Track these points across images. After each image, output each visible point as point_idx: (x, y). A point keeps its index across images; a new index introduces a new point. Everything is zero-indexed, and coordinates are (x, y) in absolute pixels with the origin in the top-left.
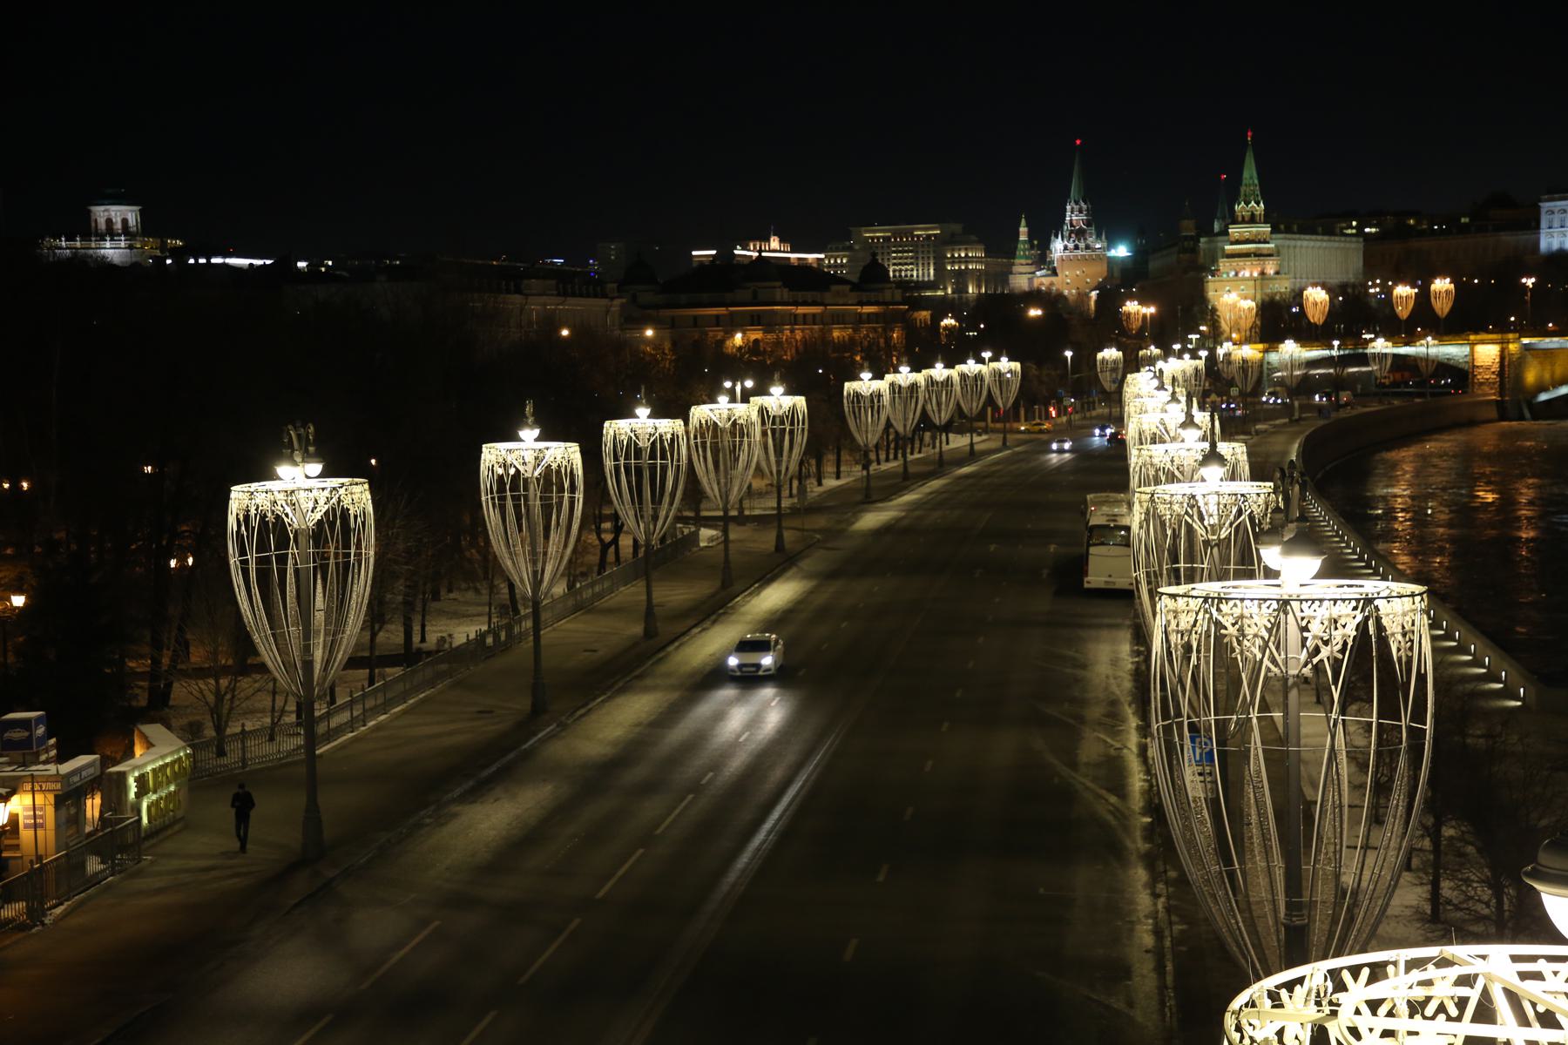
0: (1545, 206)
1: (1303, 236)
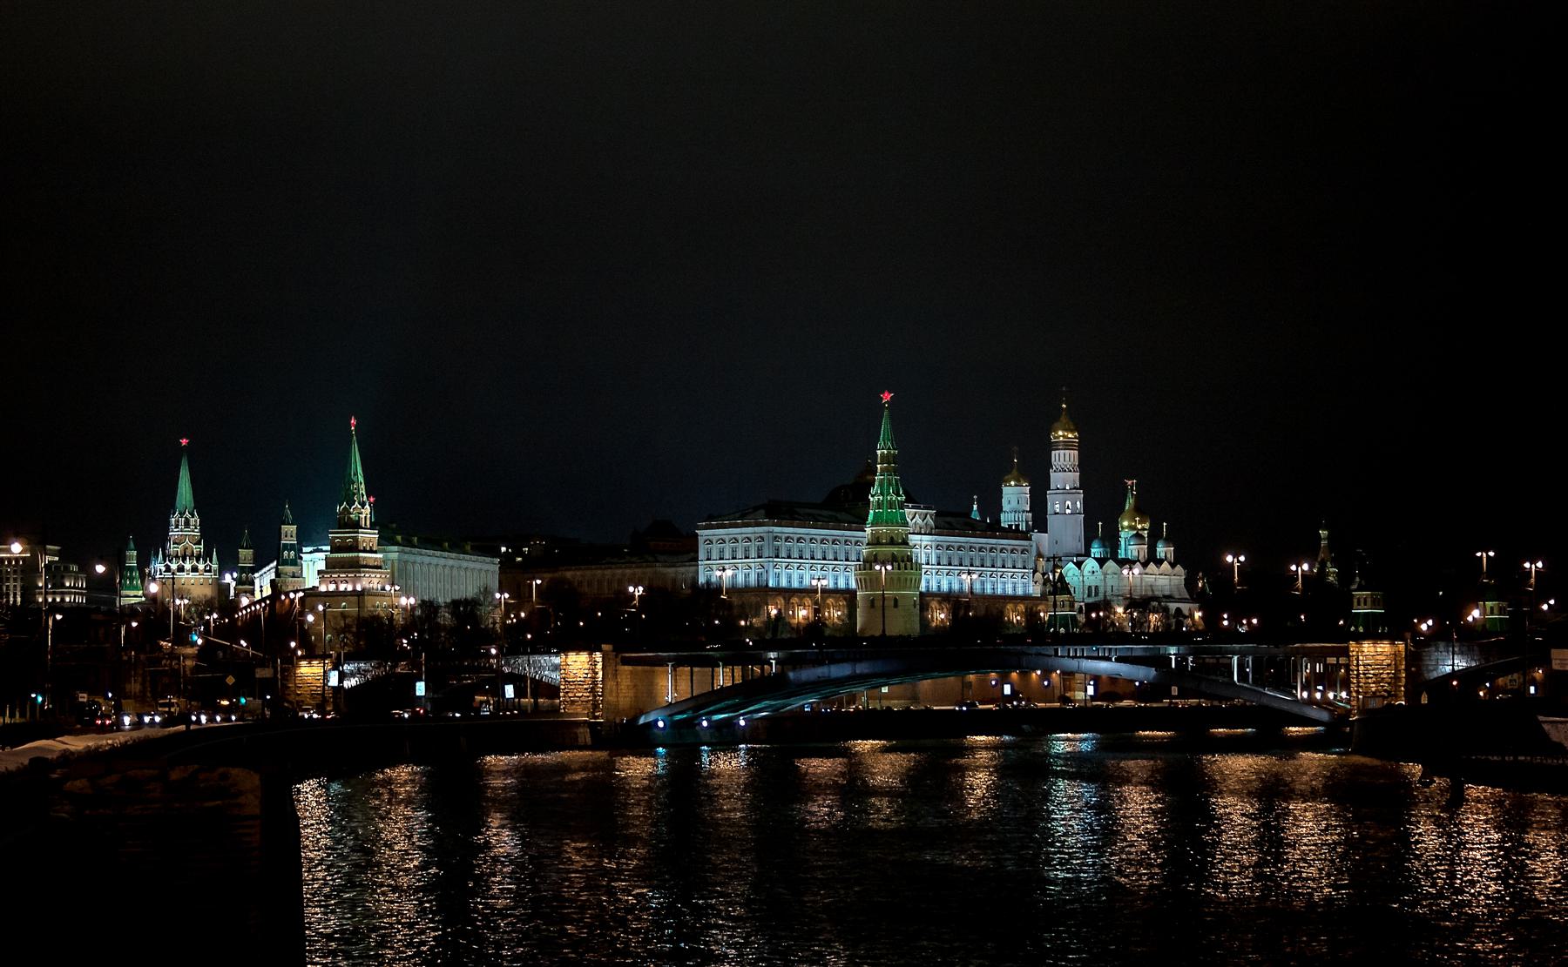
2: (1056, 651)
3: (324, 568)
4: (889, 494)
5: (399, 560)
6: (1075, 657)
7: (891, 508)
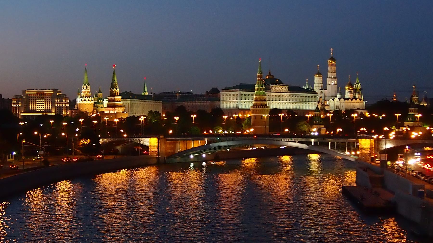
0: (222, 93)
2: (282, 139)
4: (260, 87)
5: (130, 103)
6: (287, 141)
7: (261, 91)
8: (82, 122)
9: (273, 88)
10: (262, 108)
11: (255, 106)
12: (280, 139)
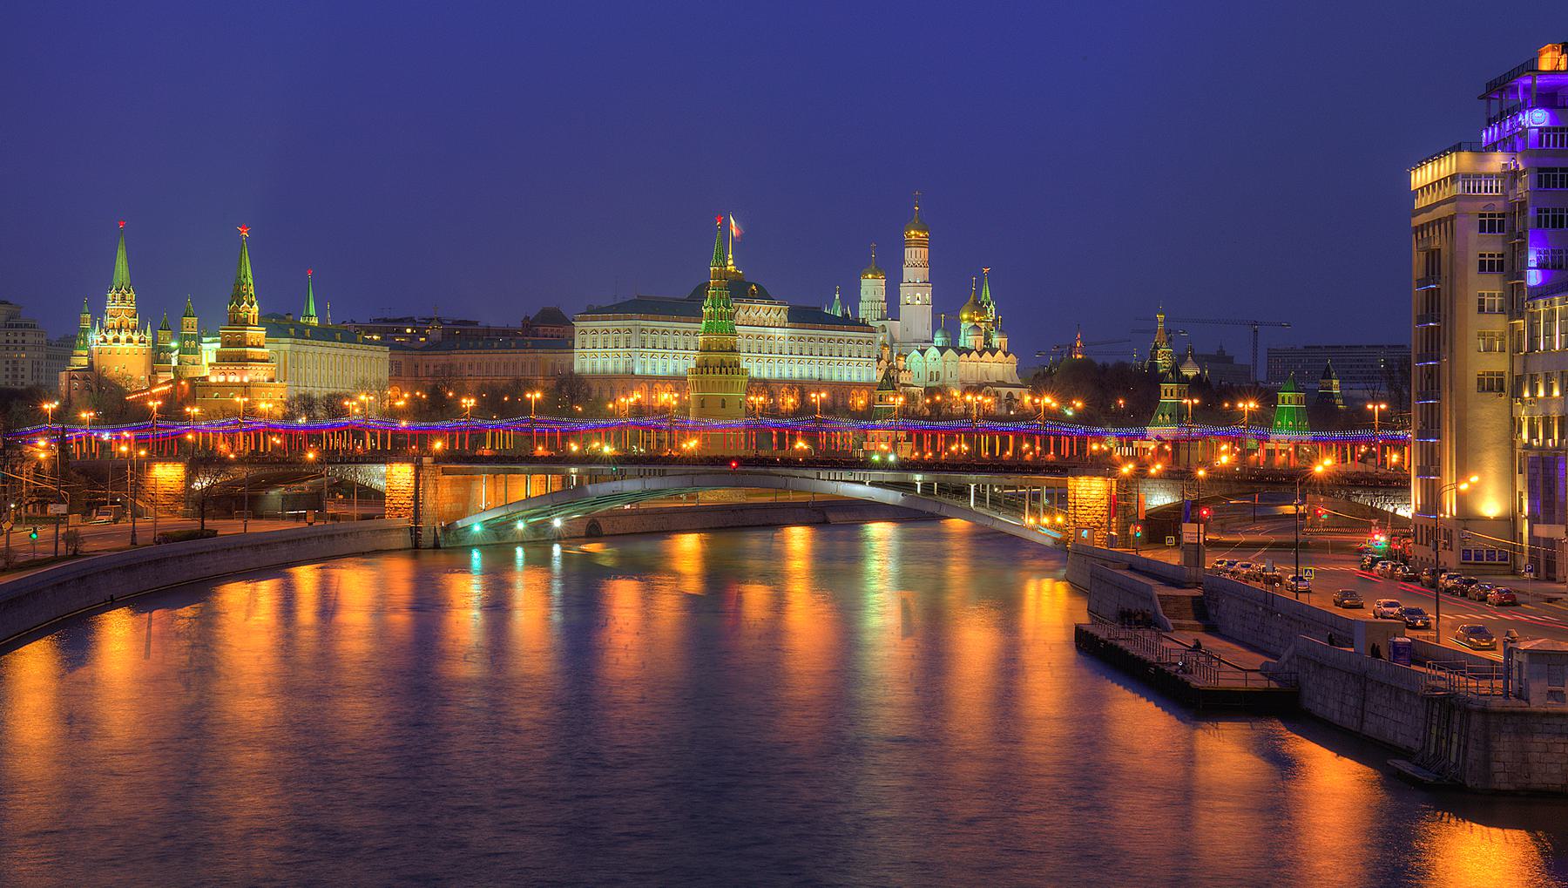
0: (579, 325)
1: (315, 342)
3: (214, 361)
6: (835, 480)
8: (155, 409)
9: (741, 313)
10: (724, 375)
11: (703, 367)
12: (812, 473)
